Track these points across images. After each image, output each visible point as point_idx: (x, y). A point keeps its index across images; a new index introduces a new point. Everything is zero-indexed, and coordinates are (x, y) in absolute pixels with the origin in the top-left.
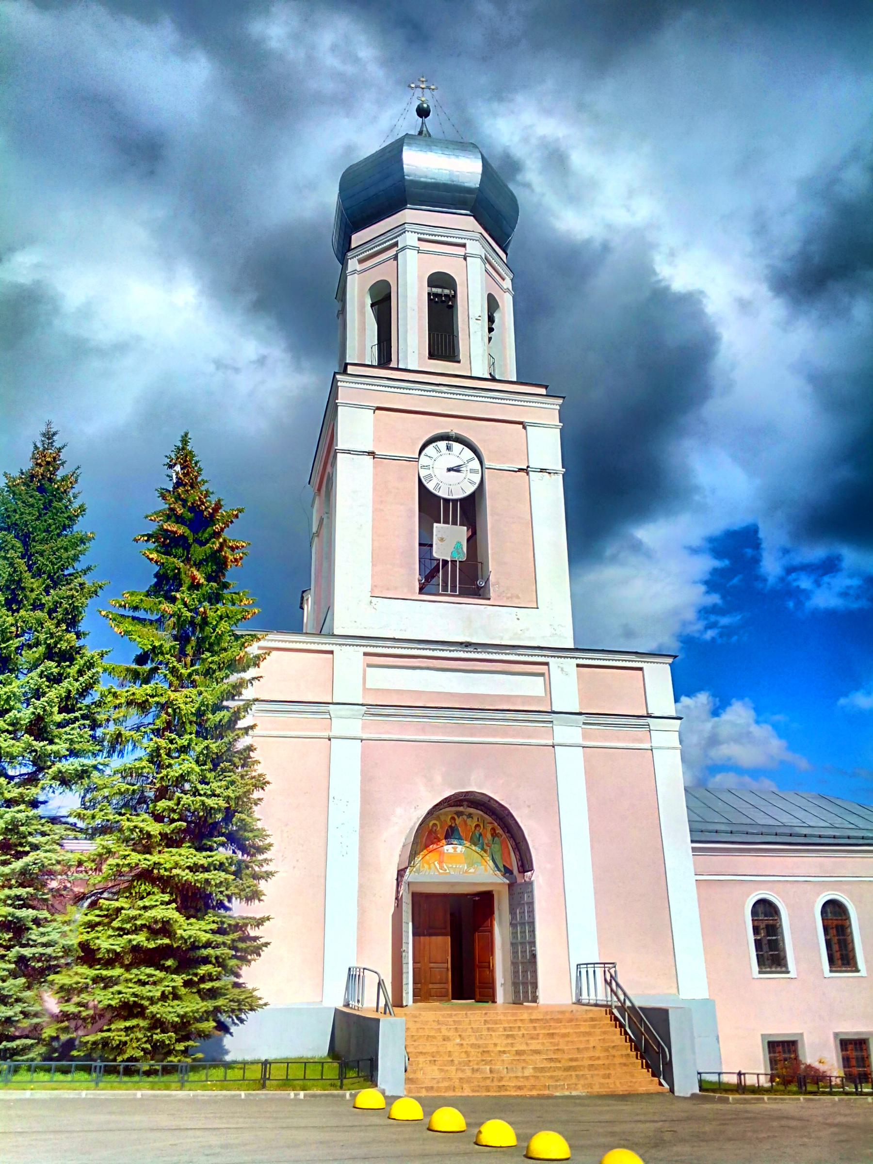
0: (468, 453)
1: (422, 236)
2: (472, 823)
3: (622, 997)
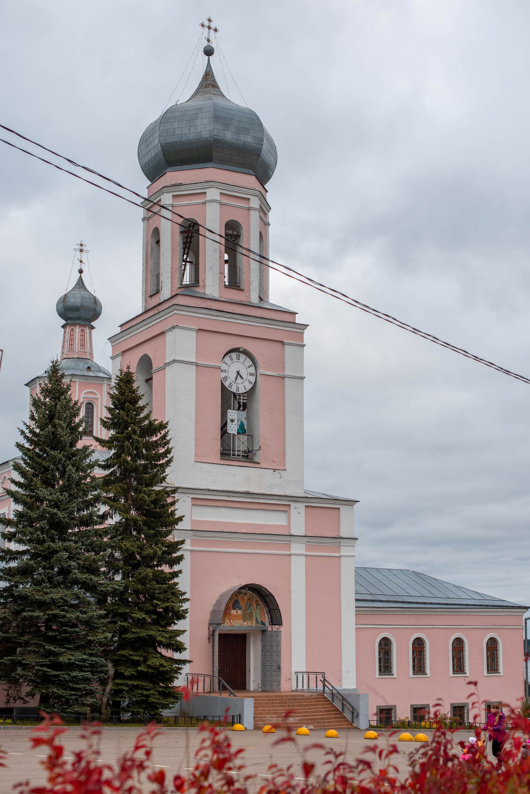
0: (248, 362)
2: (246, 598)
3: (331, 688)
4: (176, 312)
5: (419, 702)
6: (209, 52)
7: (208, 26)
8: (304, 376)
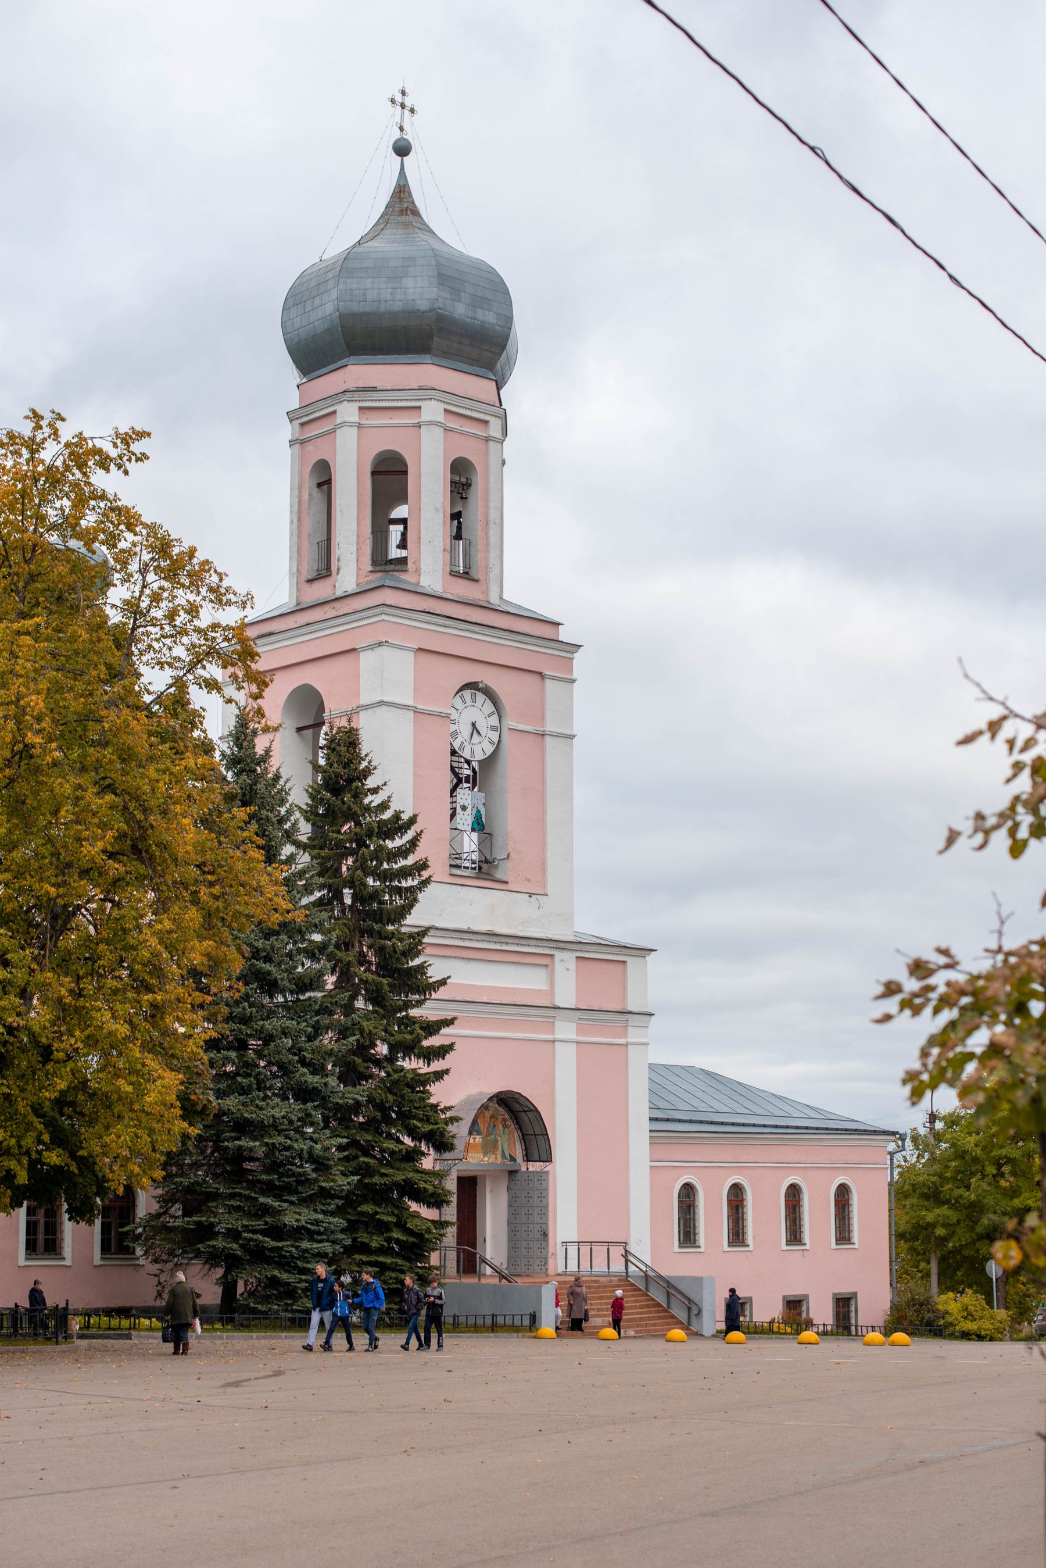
0: (489, 707)
4: (383, 617)
5: (795, 1291)
6: (402, 149)
7: (401, 103)
8: (575, 733)
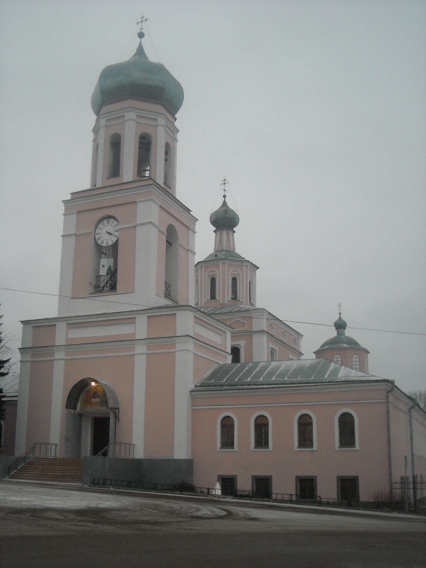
0: (115, 223)
1: (107, 118)
6: (141, 35)
